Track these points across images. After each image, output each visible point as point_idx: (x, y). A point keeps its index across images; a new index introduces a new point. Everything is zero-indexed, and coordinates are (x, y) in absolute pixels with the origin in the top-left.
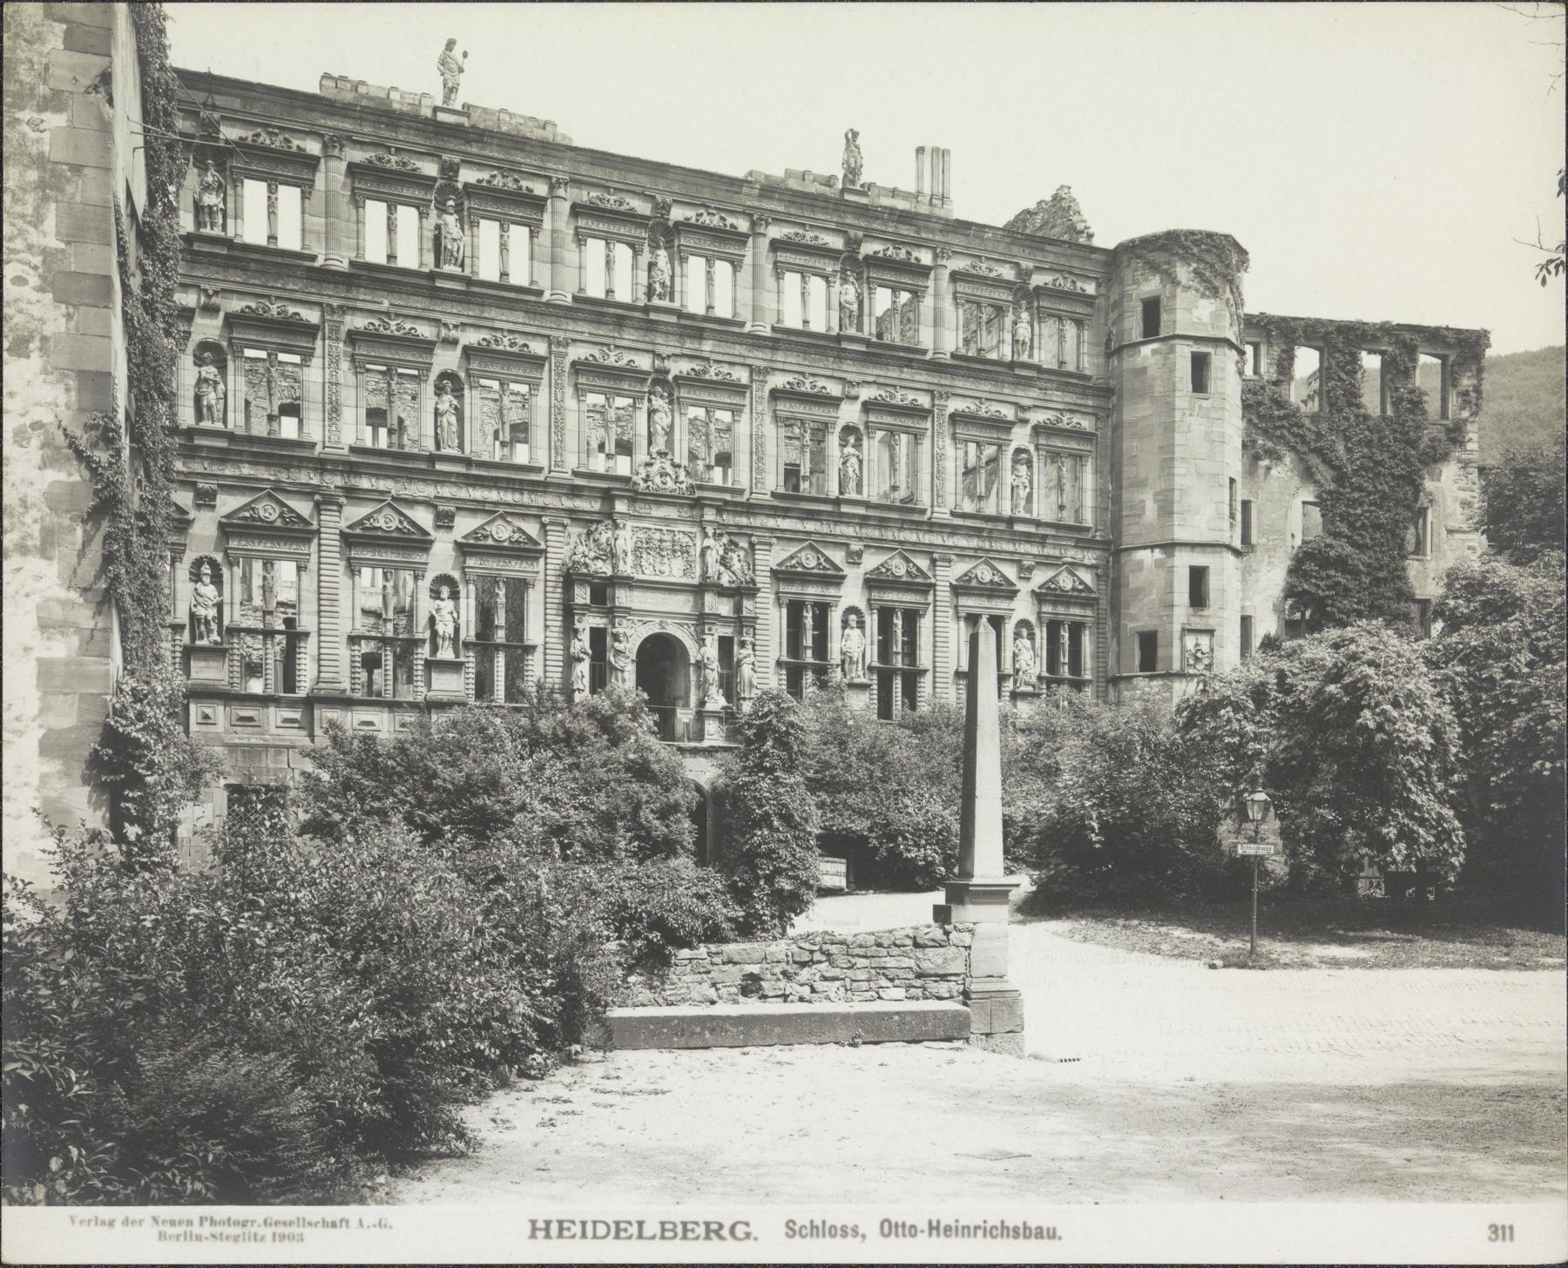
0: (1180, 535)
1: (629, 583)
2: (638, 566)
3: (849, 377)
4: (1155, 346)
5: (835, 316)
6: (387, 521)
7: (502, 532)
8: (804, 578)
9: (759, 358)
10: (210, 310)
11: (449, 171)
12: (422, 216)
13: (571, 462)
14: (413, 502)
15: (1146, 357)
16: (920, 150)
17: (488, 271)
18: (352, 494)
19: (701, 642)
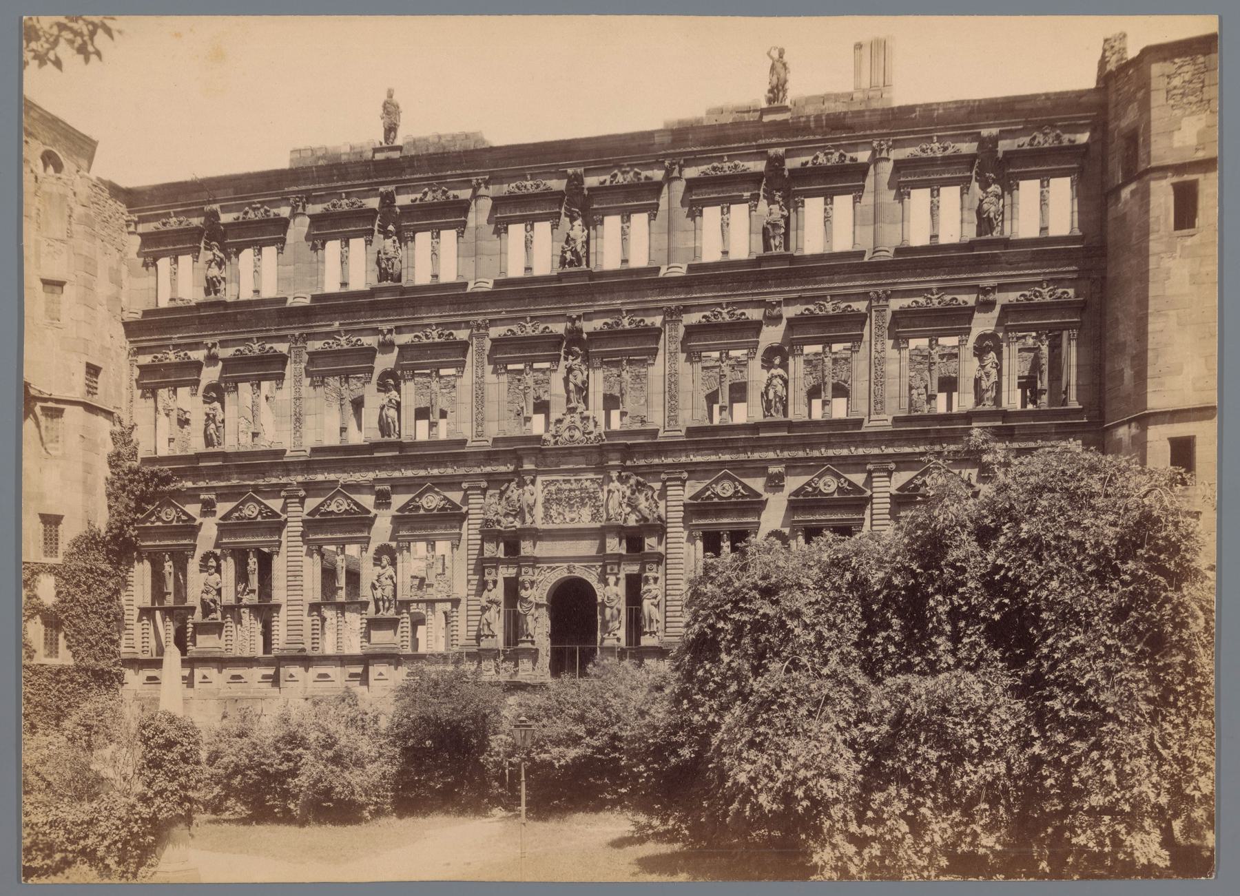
0: (1155, 402)
1: (536, 535)
2: (547, 516)
3: (769, 298)
4: (1133, 186)
5: (758, 240)
6: (338, 506)
7: (431, 501)
8: (720, 508)
9: (671, 300)
10: (212, 359)
11: (388, 199)
12: (369, 243)
13: (493, 430)
14: (357, 488)
15: (1126, 203)
16: (859, 46)
17: (422, 277)
18: (312, 488)
19: (605, 582)
